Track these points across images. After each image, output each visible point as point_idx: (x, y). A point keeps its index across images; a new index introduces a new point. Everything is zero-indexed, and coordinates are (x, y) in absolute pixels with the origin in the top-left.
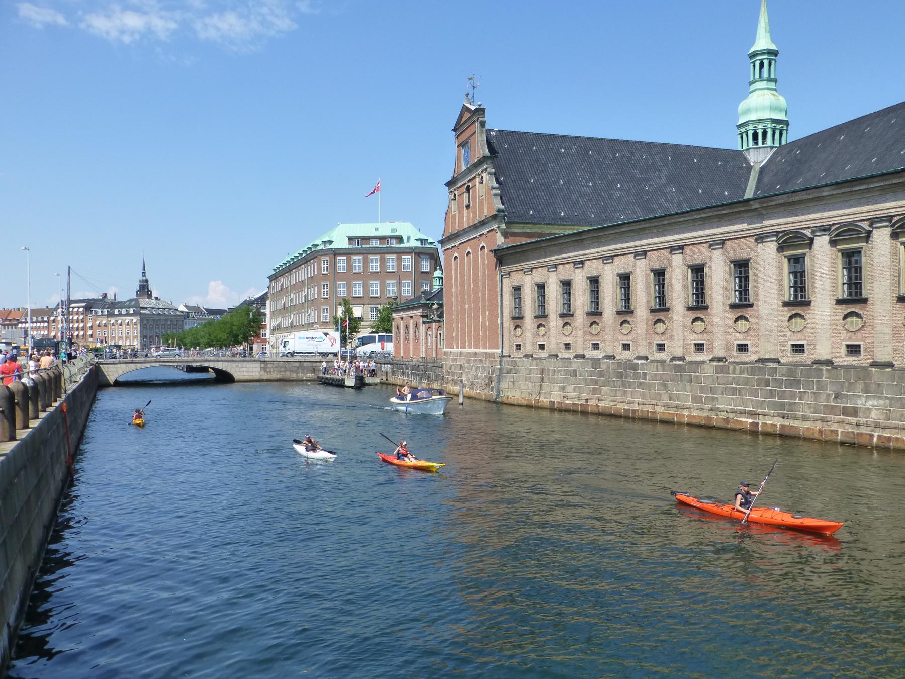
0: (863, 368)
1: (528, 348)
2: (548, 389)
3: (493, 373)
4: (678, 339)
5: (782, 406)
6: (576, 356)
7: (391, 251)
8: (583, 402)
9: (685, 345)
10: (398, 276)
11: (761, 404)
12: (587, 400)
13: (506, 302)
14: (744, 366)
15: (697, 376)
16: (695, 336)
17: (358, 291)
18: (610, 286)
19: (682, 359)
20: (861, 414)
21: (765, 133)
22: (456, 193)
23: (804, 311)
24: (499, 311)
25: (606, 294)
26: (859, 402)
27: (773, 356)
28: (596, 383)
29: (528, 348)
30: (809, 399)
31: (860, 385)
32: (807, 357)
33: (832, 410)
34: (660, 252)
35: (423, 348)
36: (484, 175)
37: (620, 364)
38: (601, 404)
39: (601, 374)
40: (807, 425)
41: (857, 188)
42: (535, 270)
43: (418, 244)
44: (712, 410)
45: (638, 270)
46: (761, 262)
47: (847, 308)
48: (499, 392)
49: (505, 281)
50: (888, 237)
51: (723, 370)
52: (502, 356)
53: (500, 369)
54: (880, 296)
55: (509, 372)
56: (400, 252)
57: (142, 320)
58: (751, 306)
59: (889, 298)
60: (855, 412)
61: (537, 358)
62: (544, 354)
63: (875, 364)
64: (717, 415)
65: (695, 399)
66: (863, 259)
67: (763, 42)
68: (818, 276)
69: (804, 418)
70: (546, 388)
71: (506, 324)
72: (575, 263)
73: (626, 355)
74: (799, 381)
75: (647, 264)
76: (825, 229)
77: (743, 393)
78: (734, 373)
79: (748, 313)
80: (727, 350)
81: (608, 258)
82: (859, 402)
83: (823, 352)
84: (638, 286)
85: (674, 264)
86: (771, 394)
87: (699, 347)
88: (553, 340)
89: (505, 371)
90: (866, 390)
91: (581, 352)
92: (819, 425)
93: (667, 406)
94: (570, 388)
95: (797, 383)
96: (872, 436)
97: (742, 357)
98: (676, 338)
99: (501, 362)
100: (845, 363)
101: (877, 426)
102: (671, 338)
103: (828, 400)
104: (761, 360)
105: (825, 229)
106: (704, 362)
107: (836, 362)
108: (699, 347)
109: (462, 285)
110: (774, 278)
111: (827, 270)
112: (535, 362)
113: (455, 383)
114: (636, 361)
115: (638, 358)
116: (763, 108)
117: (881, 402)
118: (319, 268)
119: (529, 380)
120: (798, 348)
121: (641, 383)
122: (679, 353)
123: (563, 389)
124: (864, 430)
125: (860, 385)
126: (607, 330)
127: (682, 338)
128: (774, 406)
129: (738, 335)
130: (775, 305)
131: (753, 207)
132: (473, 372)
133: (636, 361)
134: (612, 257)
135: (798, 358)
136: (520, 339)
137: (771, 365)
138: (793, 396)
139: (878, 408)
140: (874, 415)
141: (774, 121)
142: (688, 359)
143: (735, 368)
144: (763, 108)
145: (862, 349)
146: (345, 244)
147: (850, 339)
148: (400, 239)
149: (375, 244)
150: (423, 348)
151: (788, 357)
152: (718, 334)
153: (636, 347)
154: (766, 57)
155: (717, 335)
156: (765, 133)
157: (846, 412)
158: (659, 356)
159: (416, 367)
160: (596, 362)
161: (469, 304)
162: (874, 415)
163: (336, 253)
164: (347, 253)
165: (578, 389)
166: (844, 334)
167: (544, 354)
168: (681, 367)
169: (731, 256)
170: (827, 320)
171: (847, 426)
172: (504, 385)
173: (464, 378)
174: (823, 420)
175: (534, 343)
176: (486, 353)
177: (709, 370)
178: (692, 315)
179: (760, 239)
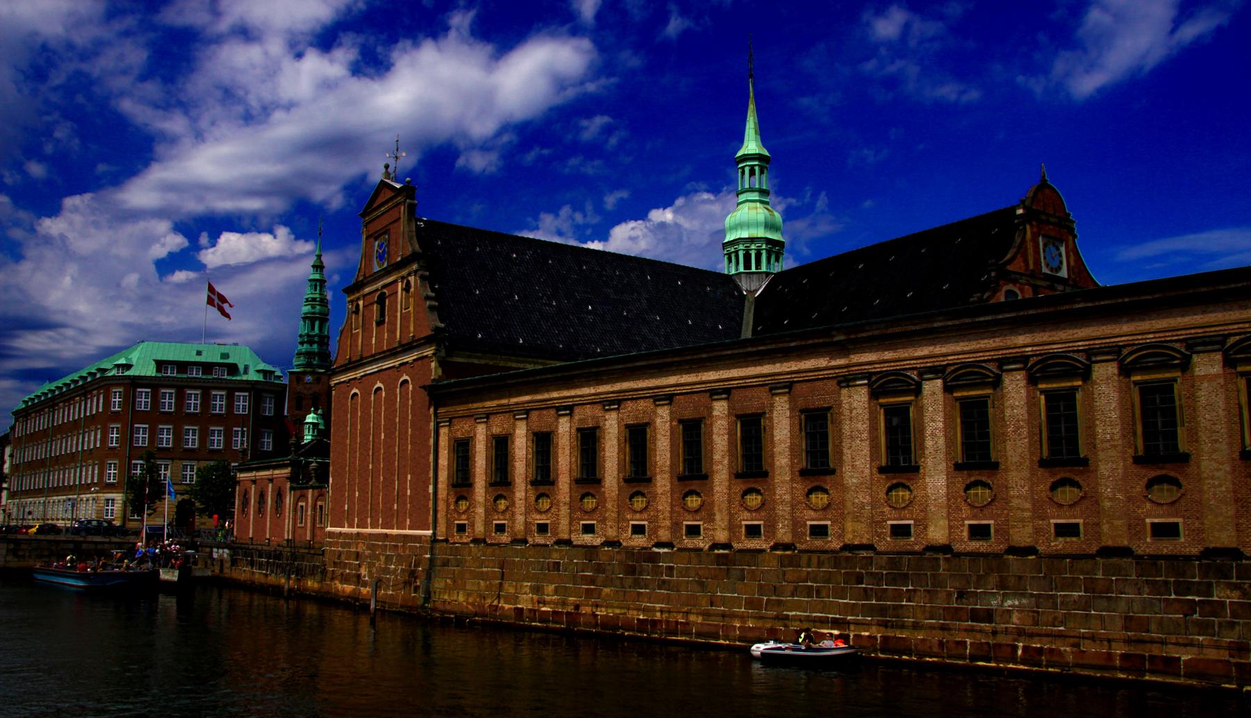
0: (997, 556)
2: (512, 590)
3: (417, 565)
4: (721, 519)
5: (882, 610)
7: (220, 384)
8: (570, 609)
9: (732, 527)
10: (229, 420)
11: (852, 609)
12: (577, 607)
13: (443, 461)
14: (823, 557)
15: (753, 571)
16: (746, 514)
17: (166, 438)
18: (615, 442)
19: (727, 546)
20: (998, 619)
22: (361, 303)
23: (909, 479)
24: (431, 474)
25: (607, 454)
26: (994, 602)
27: (865, 541)
28: (592, 581)
29: (479, 528)
31: (993, 579)
32: (914, 543)
33: (955, 614)
34: (695, 397)
35: (288, 524)
36: (412, 279)
37: (630, 552)
39: (599, 569)
41: (982, 319)
42: (492, 417)
43: (260, 378)
44: (777, 618)
45: (658, 421)
46: (847, 413)
47: (970, 476)
49: (444, 431)
50: (1023, 383)
51: (793, 562)
53: (431, 560)
54: (1015, 459)
55: (446, 563)
56: (232, 390)
58: (833, 472)
59: (1027, 463)
60: (988, 616)
61: (492, 545)
63: (1013, 550)
64: (786, 626)
65: (750, 603)
66: (991, 411)
68: (929, 432)
69: (916, 626)
70: (509, 588)
71: (442, 493)
72: (558, 409)
73: (639, 541)
74: (906, 575)
75: (671, 413)
76: (937, 371)
77: (824, 594)
78: (809, 566)
79: (828, 482)
80: (794, 533)
82: (994, 602)
83: (937, 533)
84: (659, 443)
85: (715, 413)
86: (866, 594)
87: (753, 531)
88: (520, 519)
89: (439, 562)
90: (1002, 585)
91: (566, 537)
92: (937, 636)
93: (706, 614)
95: (904, 579)
96: (1015, 648)
97: (819, 543)
98: (718, 517)
99: (432, 549)
100: (969, 549)
101: (1020, 633)
102: (710, 518)
103: (948, 601)
104: (846, 547)
105: (937, 371)
106: (762, 551)
107: (957, 547)
108: (753, 531)
109: (365, 434)
110: (865, 435)
111: (941, 425)
112: (490, 550)
113: (345, 579)
114: (655, 550)
116: (757, 225)
117: (1024, 601)
118: (107, 403)
120: (901, 531)
121: (664, 581)
122: (722, 536)
124: (1002, 639)
125: (993, 579)
126: (609, 505)
127: (727, 518)
128: (870, 610)
129: (812, 513)
130: (867, 471)
131: (836, 339)
132: (381, 563)
133: (655, 550)
134: (619, 402)
135: (901, 543)
136: (464, 517)
137: (864, 554)
138: (898, 596)
139: (1021, 609)
141: (768, 241)
142: (736, 545)
143: (810, 559)
144: (757, 225)
145: (992, 531)
146: (150, 371)
147: (975, 517)
148: (233, 369)
149: (196, 374)
150: (288, 524)
151: (886, 543)
153: (655, 531)
155: (781, 513)
157: (975, 616)
158: (689, 542)
160: (590, 550)
161: (376, 460)
164: (152, 384)
166: (966, 511)
167: (505, 538)
168: (726, 560)
169: (801, 403)
170: (943, 491)
171: (978, 636)
173: (363, 571)
174: (943, 628)
175: (487, 523)
176: (405, 536)
178: (740, 487)
179: (846, 380)
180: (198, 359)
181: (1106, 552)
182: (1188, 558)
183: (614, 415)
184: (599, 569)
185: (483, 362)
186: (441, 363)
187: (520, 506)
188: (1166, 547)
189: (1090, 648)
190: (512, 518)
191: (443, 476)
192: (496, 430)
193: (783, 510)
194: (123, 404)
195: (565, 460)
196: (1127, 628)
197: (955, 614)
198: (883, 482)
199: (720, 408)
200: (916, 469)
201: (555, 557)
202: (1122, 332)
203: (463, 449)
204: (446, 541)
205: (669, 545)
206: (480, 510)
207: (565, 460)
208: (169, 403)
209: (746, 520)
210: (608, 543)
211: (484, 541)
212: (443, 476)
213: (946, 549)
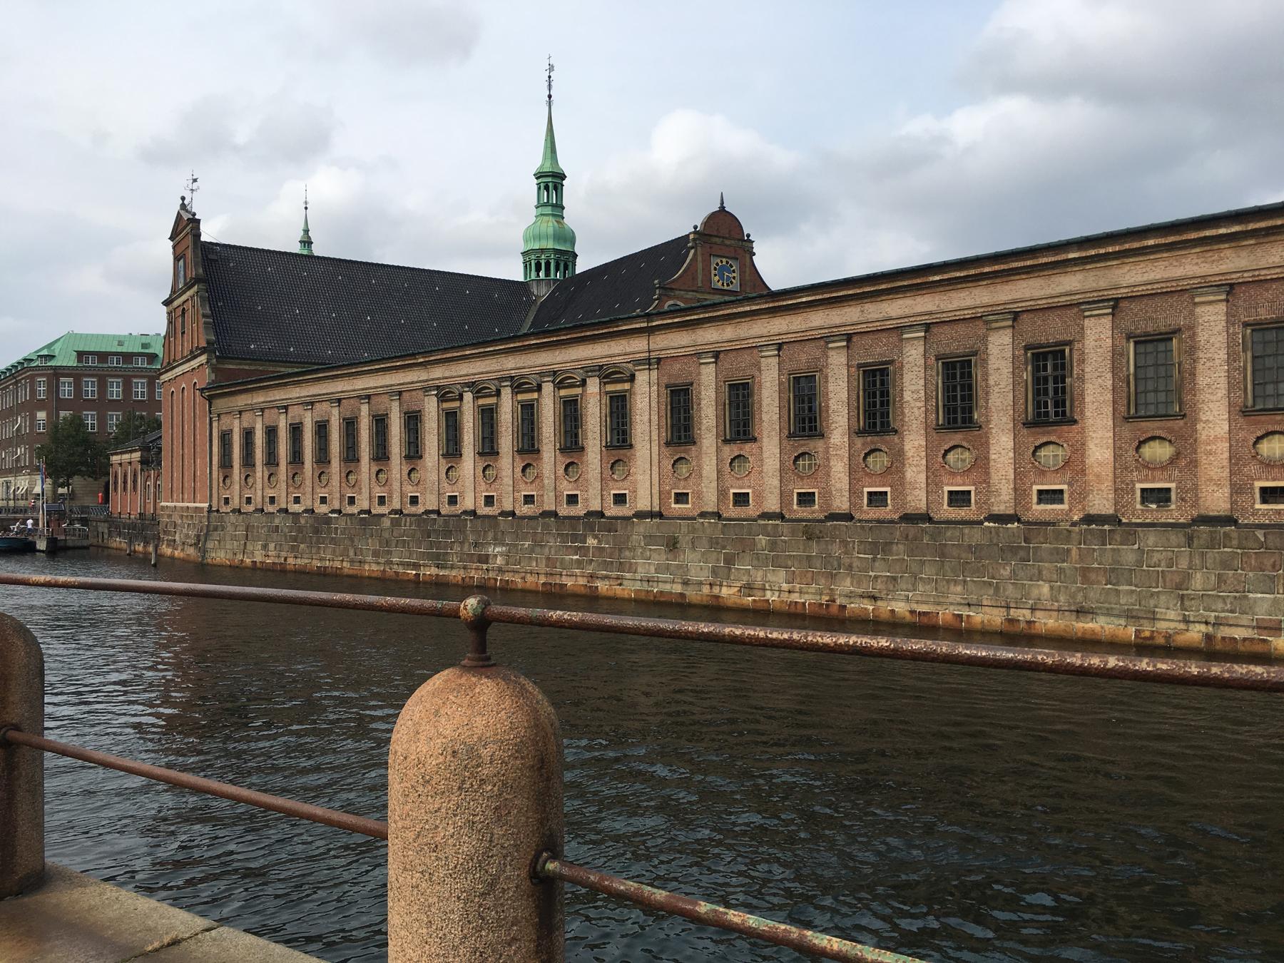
0: (495, 517)
1: (235, 503)
4: (365, 491)
5: (437, 557)
6: (234, 511)
8: (282, 560)
19: (369, 512)
21: (548, 264)
29: (235, 503)
30: (457, 548)
38: (299, 561)
39: (300, 530)
40: (454, 573)
48: (204, 551)
52: (210, 510)
55: (216, 529)
60: (484, 559)
62: (251, 508)
65: (376, 554)
69: (452, 567)
70: (250, 547)
81: (308, 404)
83: (468, 503)
86: (431, 545)
93: (352, 561)
94: (272, 546)
95: (448, 534)
101: (500, 570)
106: (383, 515)
107: (479, 512)
115: (333, 511)
118: (33, 392)
119: (234, 538)
123: (265, 547)
124: (491, 575)
125: (491, 535)
134: (312, 404)
139: (502, 554)
140: (499, 561)
146: (71, 361)
152: (548, 481)
154: (550, 179)
156: (548, 264)
159: (133, 526)
162: (499, 561)
163: (58, 372)
164: (76, 375)
165: (279, 547)
166: (483, 486)
167: (251, 508)
172: (210, 545)
173: (177, 538)
177: (386, 523)
180: (120, 349)
181: (546, 514)
182: (579, 518)
183: (309, 413)
184: (300, 530)
185: (253, 368)
186: (214, 369)
189: (529, 578)
190: (255, 494)
192: (245, 425)
194: (49, 391)
196: (547, 566)
199: (365, 409)
200: (583, 449)
201: (277, 521)
202: (684, 343)
203: (226, 438)
204: (218, 511)
205: (339, 512)
206: (237, 487)
209: (379, 492)
210: (306, 511)
211: (239, 511)
213: (474, 513)
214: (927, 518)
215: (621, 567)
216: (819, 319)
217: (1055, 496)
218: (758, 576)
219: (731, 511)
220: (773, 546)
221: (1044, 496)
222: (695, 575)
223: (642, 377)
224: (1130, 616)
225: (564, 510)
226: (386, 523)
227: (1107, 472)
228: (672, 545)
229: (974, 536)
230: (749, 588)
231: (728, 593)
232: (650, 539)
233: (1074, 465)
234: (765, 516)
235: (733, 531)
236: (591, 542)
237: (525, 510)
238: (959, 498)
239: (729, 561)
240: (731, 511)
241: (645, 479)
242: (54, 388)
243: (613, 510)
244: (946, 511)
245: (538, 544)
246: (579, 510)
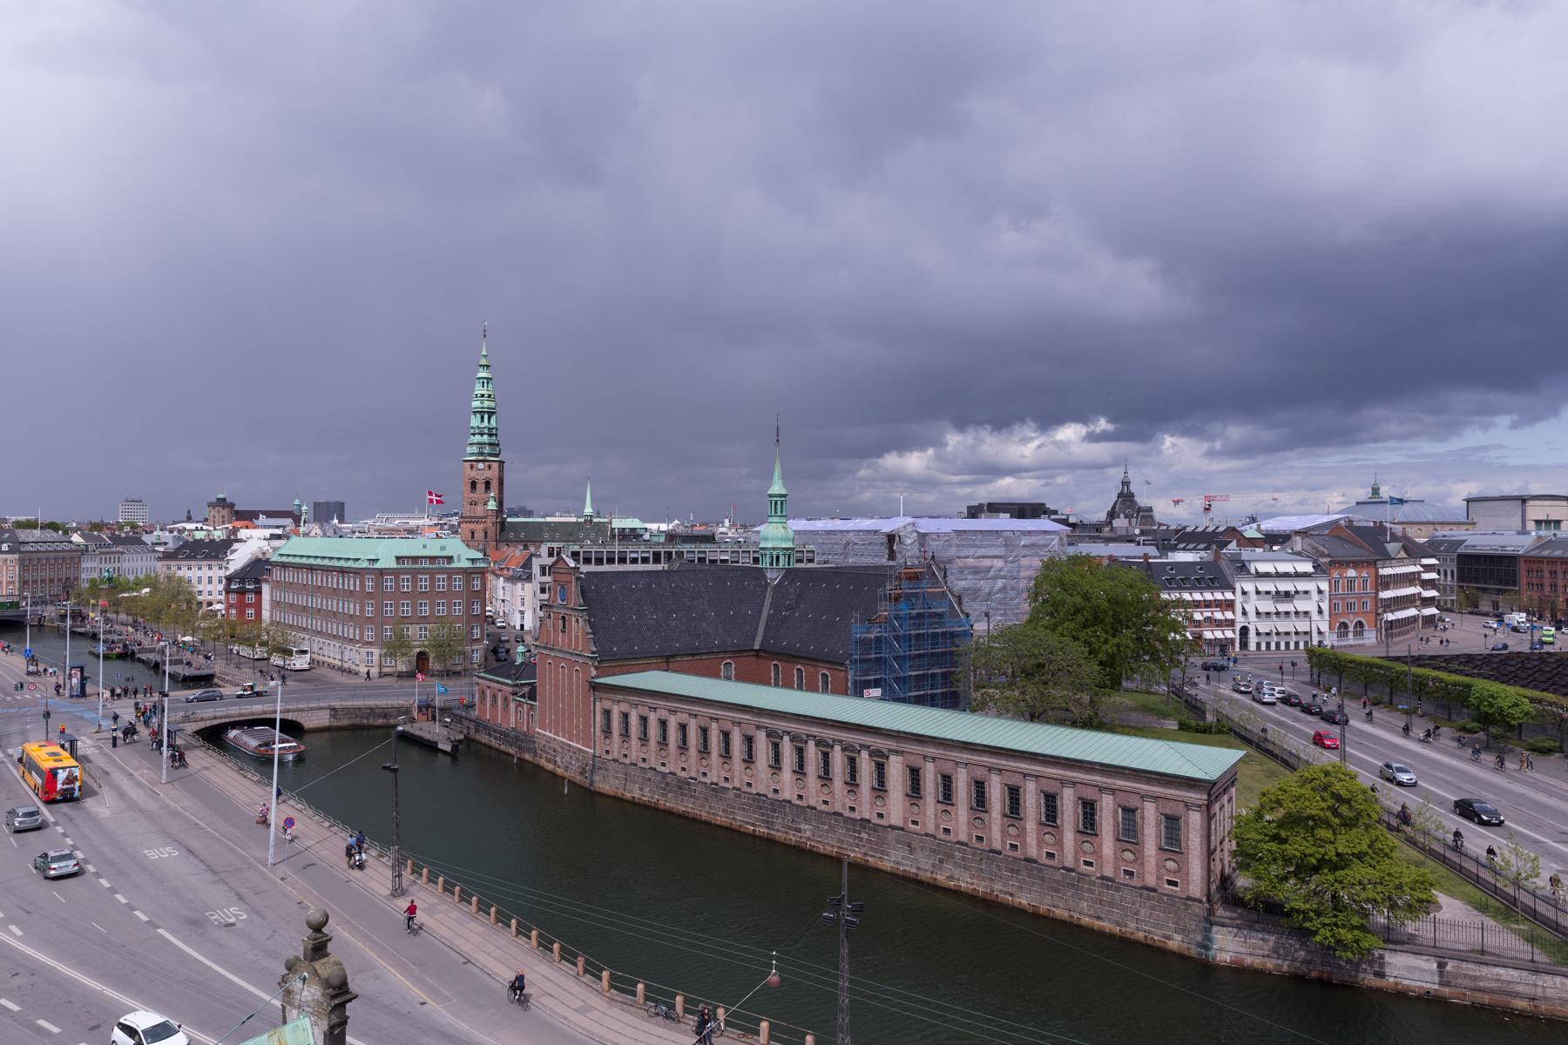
1: (615, 755)
4: (715, 773)
7: (442, 571)
10: (449, 595)
17: (407, 611)
32: (780, 797)
33: (790, 828)
35: (513, 720)
37: (679, 780)
43: (468, 565)
51: (738, 796)
56: (451, 573)
57: (21, 561)
60: (799, 830)
67: (777, 488)
70: (629, 786)
73: (683, 774)
87: (726, 779)
95: (774, 811)
113: (548, 760)
120: (776, 791)
132: (567, 759)
146: (393, 564)
148: (450, 559)
149: (426, 565)
150: (513, 720)
160: (664, 775)
177: (731, 795)
179: (758, 727)
181: (835, 814)
187: (634, 748)
188: (852, 815)
191: (598, 725)
193: (737, 774)
195: (654, 731)
197: (790, 828)
198: (770, 771)
207: (654, 731)
208: (406, 586)
212: (598, 725)
214: (1035, 861)
215: (882, 852)
216: (986, 759)
217: (1091, 864)
218: (957, 873)
219: (941, 836)
220: (963, 859)
221: (1086, 863)
222: (920, 864)
223: (893, 758)
224: (1118, 924)
225: (847, 813)
226: (731, 795)
227: (1111, 860)
228: (912, 850)
229: (1058, 875)
230: (951, 878)
231: (941, 878)
232: (898, 841)
233: (1097, 852)
234: (958, 843)
235: (944, 848)
236: (864, 835)
237: (823, 807)
238: (1050, 855)
239: (941, 861)
240: (941, 836)
241: (896, 808)
242: (379, 585)
243: (875, 820)
244: (1044, 860)
245: (832, 829)
246: (856, 816)
